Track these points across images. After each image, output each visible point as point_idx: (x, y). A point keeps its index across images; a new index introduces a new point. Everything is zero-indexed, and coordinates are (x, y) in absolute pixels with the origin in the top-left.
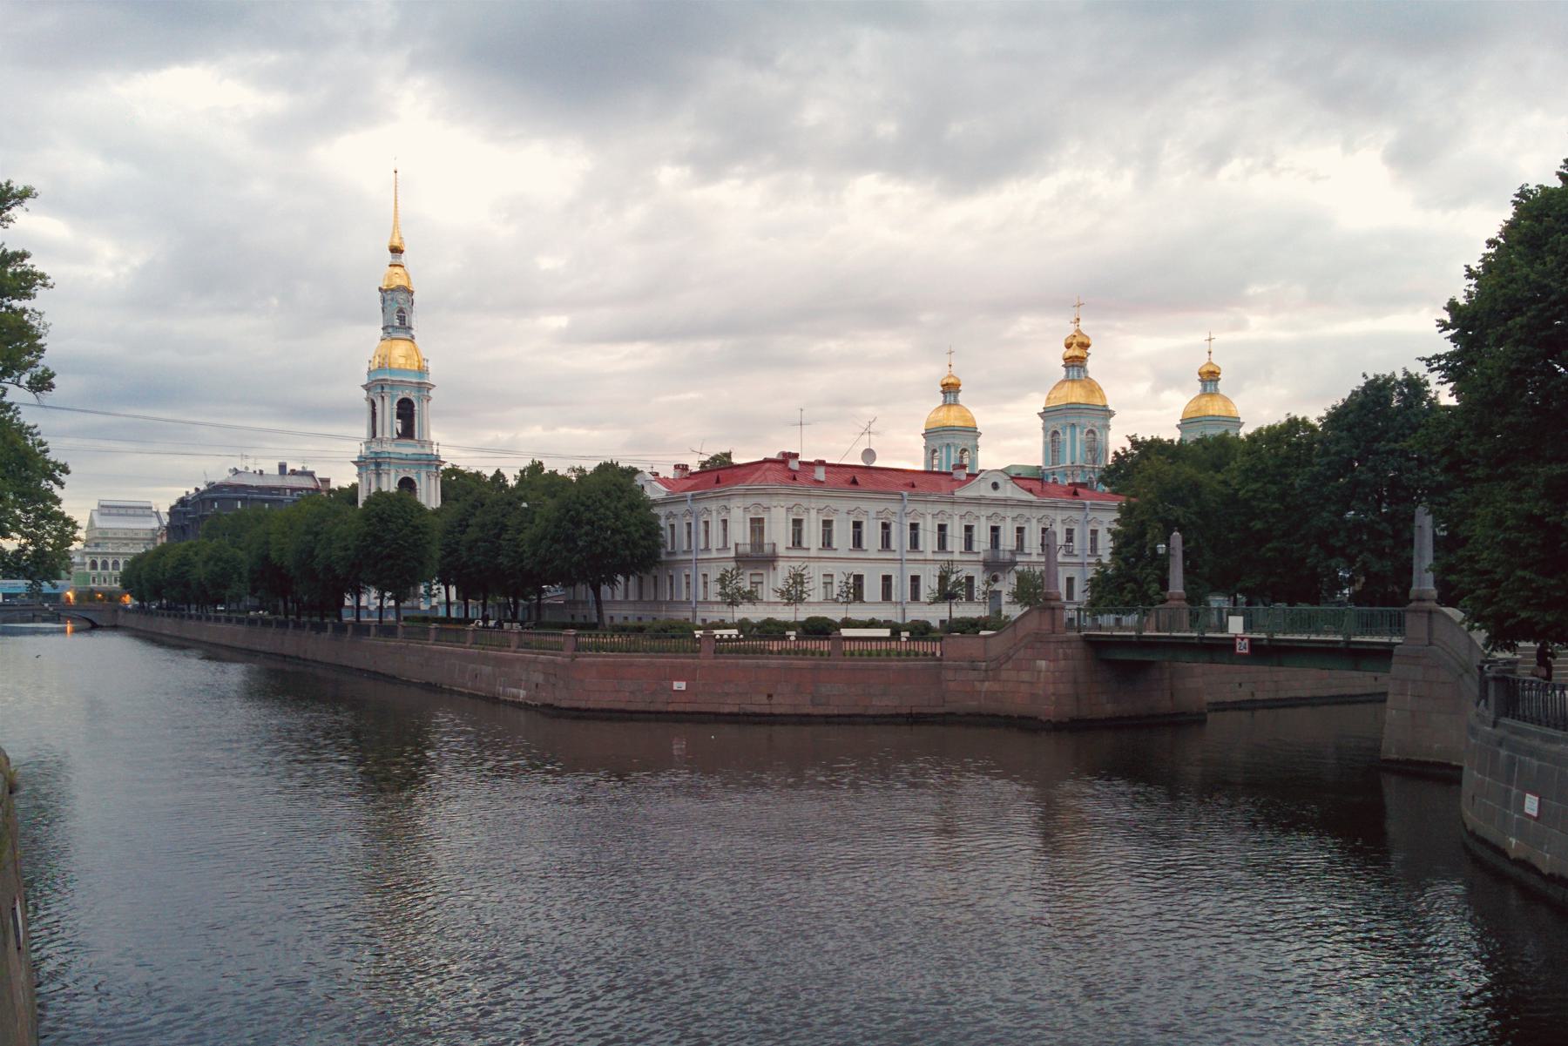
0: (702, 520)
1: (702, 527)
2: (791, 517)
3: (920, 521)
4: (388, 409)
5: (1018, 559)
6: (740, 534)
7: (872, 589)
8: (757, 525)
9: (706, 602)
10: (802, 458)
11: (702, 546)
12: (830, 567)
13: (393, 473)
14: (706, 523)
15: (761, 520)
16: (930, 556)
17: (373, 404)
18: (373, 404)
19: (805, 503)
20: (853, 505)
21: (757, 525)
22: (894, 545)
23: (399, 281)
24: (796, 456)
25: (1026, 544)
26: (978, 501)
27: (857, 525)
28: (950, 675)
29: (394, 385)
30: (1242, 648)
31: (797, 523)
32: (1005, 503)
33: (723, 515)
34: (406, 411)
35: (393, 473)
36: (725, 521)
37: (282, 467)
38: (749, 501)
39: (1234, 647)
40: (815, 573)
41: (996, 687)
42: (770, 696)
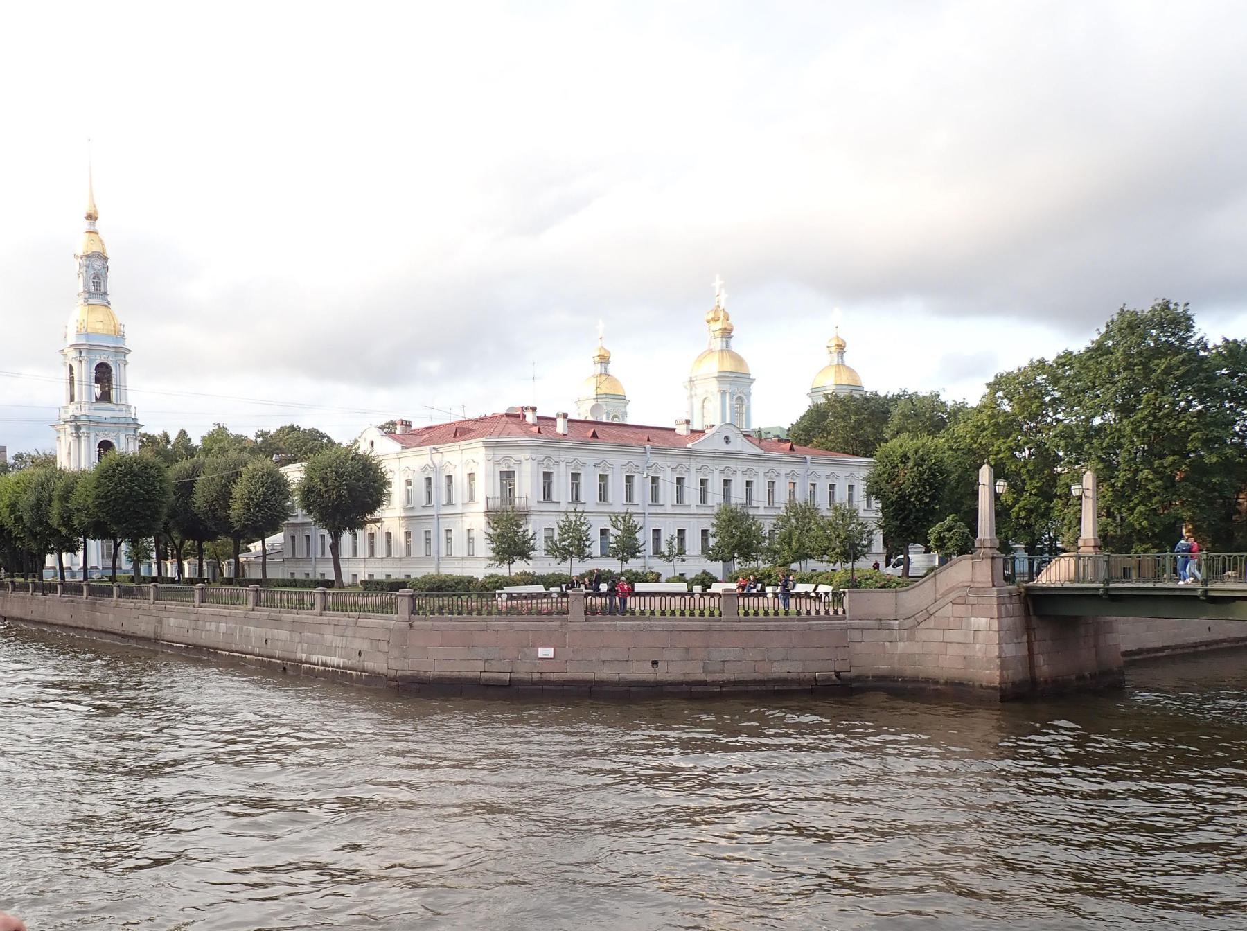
1: (444, 482)
2: (542, 470)
3: (660, 475)
4: (84, 373)
8: (508, 477)
10: (539, 413)
13: (92, 436)
16: (669, 509)
17: (71, 368)
18: (71, 368)
19: (554, 455)
20: (599, 457)
21: (508, 477)
22: (636, 499)
23: (96, 248)
24: (534, 409)
25: (754, 497)
26: (713, 455)
27: (603, 477)
28: (855, 636)
29: (90, 349)
31: (547, 475)
32: (736, 456)
34: (103, 374)
35: (92, 436)
38: (501, 454)
42: (655, 663)
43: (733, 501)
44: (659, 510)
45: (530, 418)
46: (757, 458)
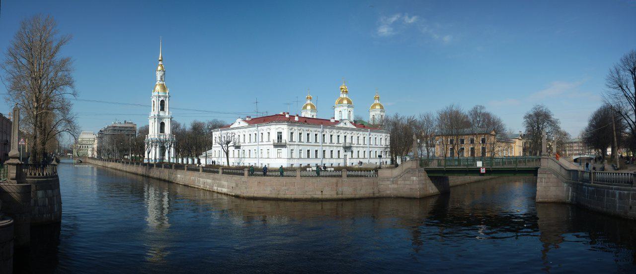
0: (260, 132)
1: (260, 135)
2: (290, 131)
5: (352, 145)
6: (274, 137)
7: (312, 154)
9: (262, 158)
11: (260, 140)
12: (301, 148)
14: (262, 133)
15: (281, 133)
28: (381, 183)
30: (483, 171)
31: (292, 133)
32: (347, 129)
33: (268, 131)
36: (269, 133)
37: (125, 121)
39: (480, 170)
40: (296, 149)
41: (396, 186)
42: (322, 192)
43: (347, 142)
44: (326, 144)
45: (287, 116)
46: (352, 130)
